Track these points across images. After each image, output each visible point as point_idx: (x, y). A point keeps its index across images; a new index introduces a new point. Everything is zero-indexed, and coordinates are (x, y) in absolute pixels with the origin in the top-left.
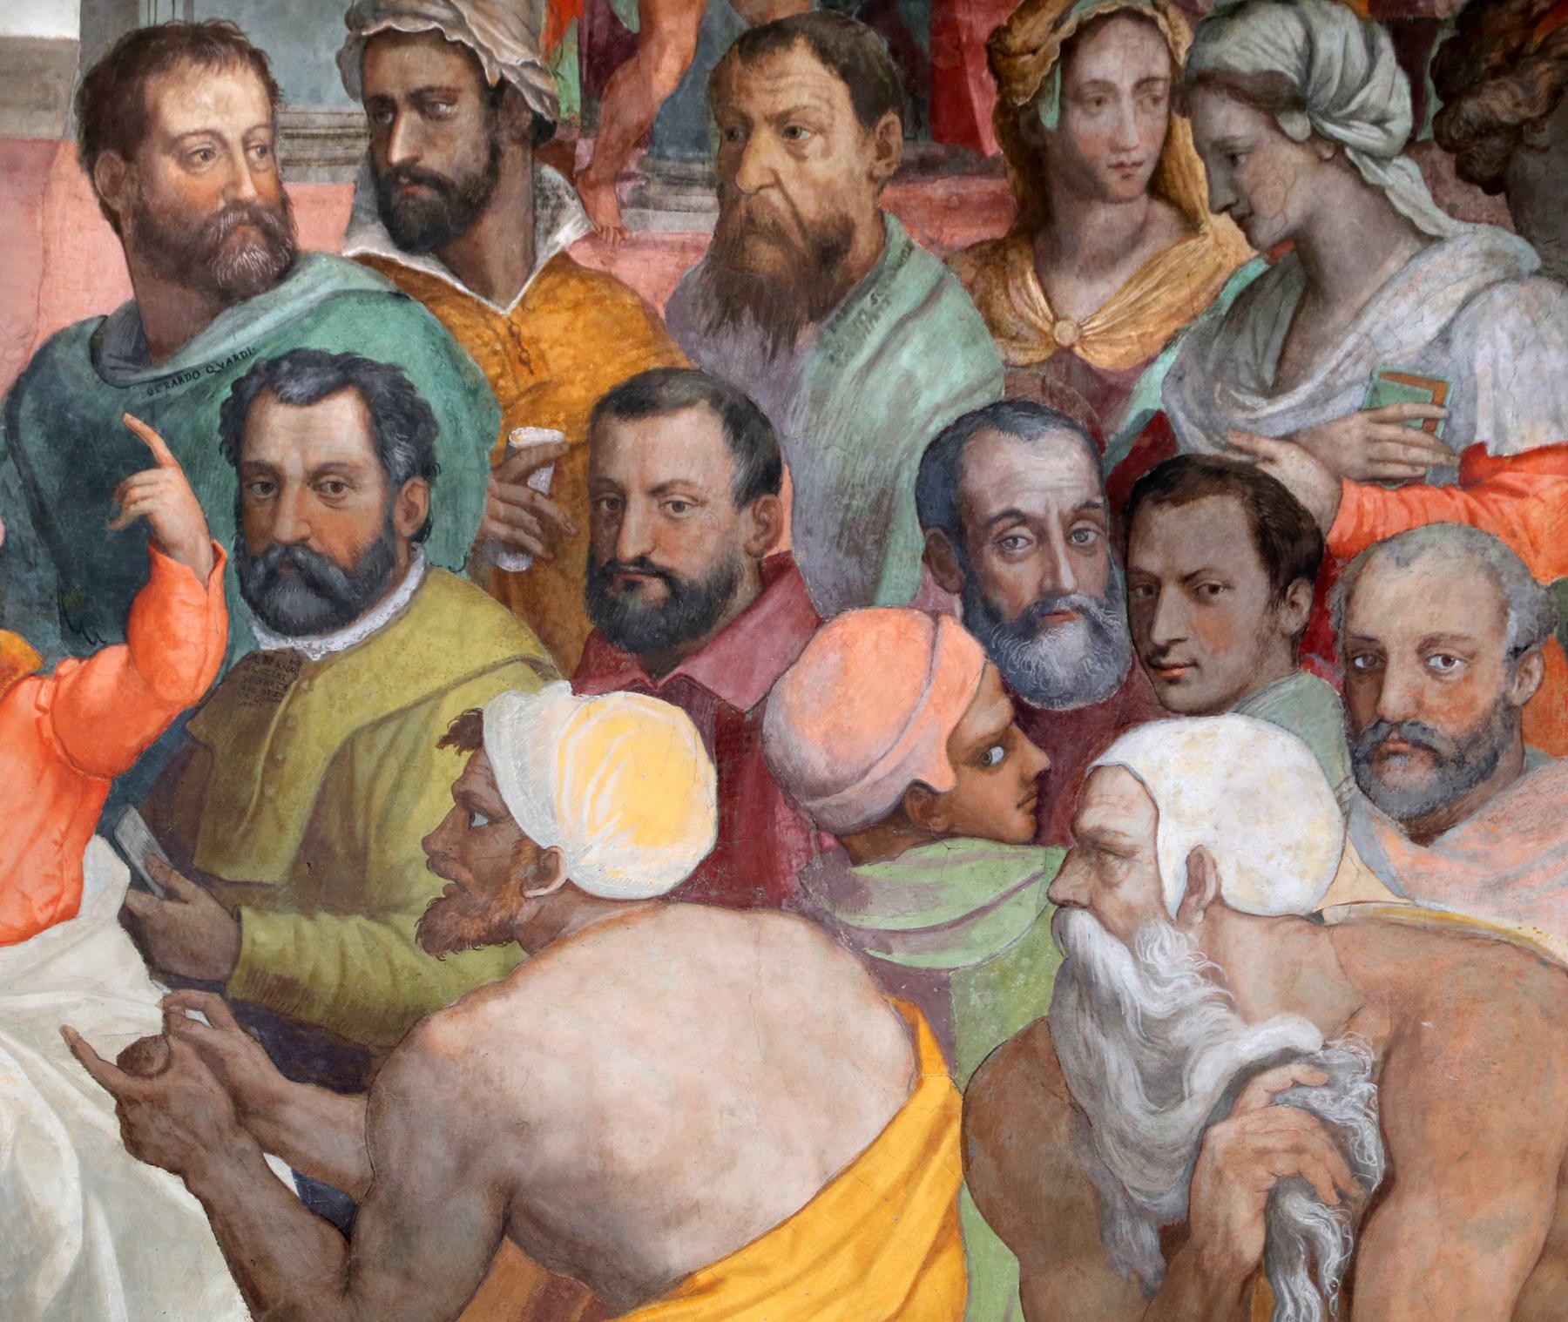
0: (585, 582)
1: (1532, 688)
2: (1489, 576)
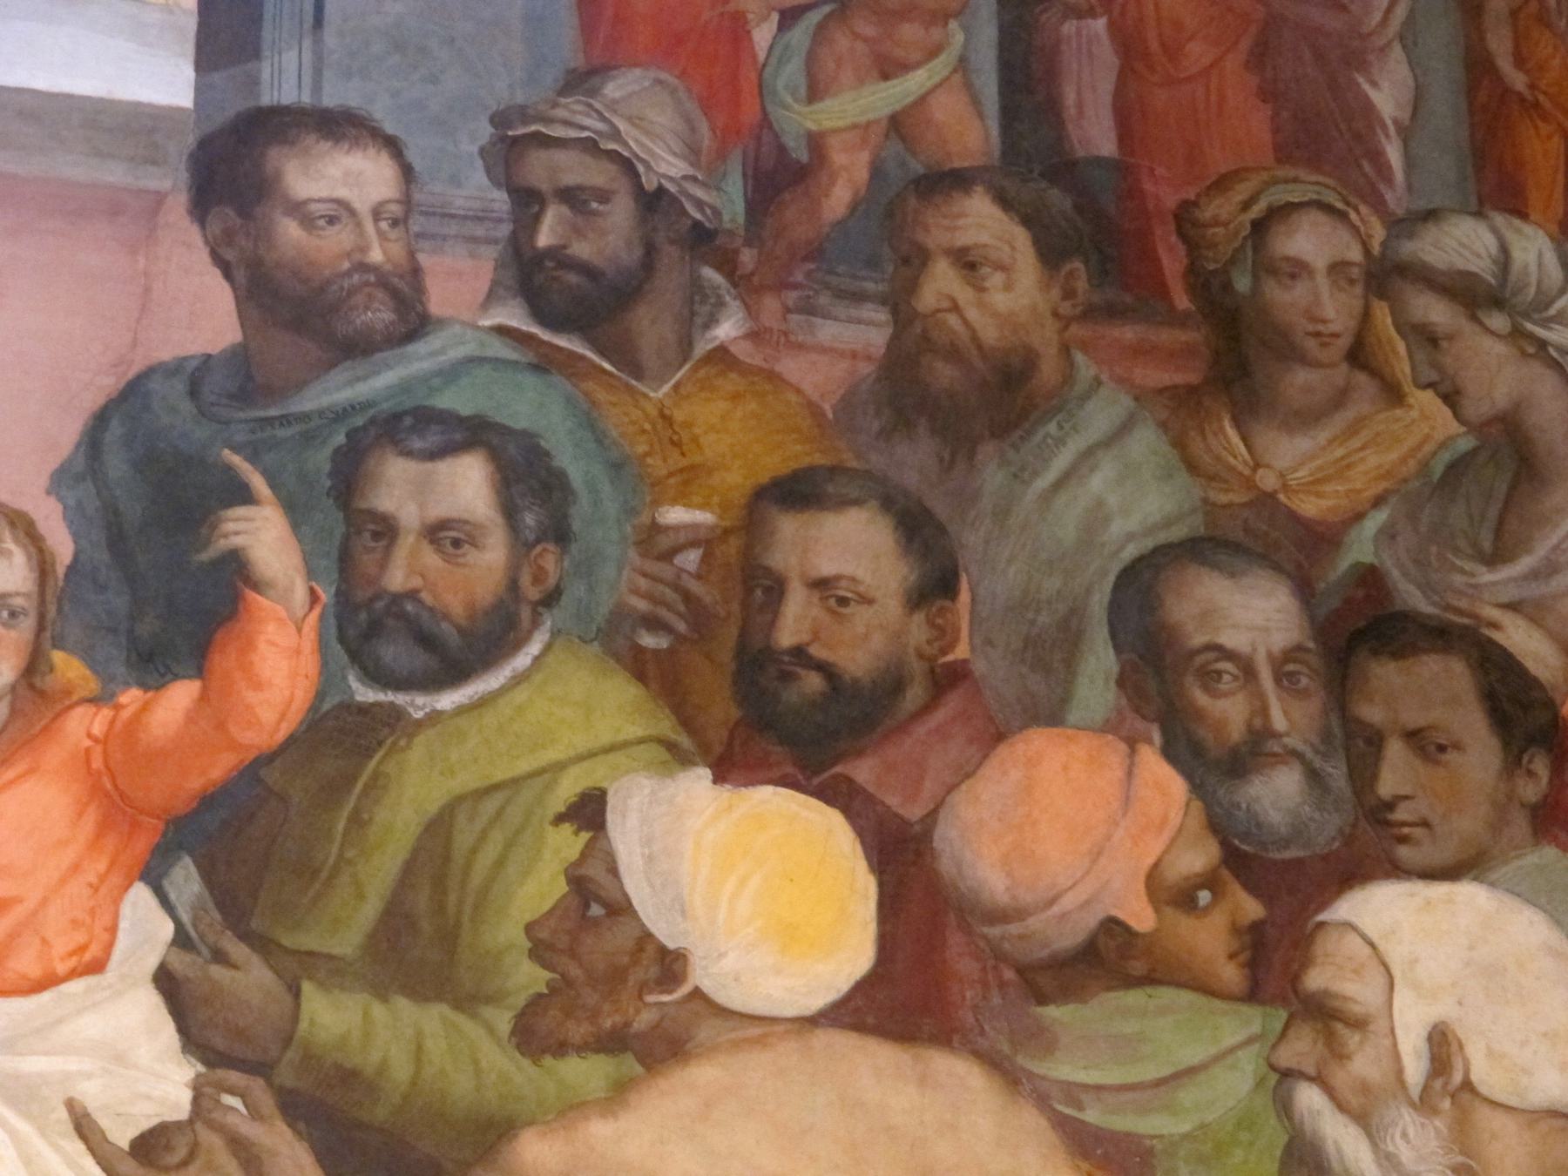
0: (733, 666)
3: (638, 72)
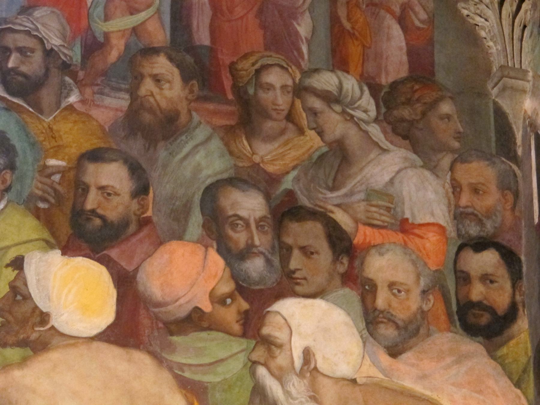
1: (431, 305)
2: (413, 264)
3: (46, 8)
